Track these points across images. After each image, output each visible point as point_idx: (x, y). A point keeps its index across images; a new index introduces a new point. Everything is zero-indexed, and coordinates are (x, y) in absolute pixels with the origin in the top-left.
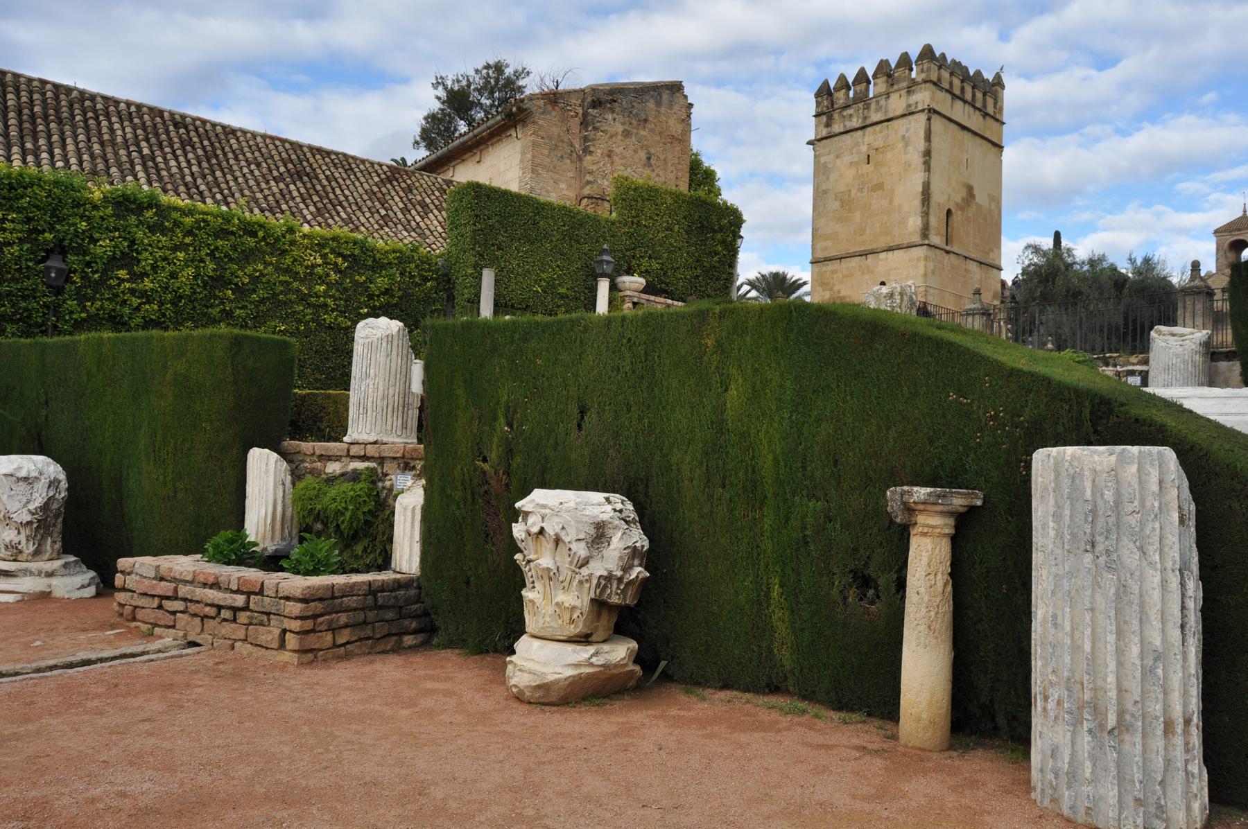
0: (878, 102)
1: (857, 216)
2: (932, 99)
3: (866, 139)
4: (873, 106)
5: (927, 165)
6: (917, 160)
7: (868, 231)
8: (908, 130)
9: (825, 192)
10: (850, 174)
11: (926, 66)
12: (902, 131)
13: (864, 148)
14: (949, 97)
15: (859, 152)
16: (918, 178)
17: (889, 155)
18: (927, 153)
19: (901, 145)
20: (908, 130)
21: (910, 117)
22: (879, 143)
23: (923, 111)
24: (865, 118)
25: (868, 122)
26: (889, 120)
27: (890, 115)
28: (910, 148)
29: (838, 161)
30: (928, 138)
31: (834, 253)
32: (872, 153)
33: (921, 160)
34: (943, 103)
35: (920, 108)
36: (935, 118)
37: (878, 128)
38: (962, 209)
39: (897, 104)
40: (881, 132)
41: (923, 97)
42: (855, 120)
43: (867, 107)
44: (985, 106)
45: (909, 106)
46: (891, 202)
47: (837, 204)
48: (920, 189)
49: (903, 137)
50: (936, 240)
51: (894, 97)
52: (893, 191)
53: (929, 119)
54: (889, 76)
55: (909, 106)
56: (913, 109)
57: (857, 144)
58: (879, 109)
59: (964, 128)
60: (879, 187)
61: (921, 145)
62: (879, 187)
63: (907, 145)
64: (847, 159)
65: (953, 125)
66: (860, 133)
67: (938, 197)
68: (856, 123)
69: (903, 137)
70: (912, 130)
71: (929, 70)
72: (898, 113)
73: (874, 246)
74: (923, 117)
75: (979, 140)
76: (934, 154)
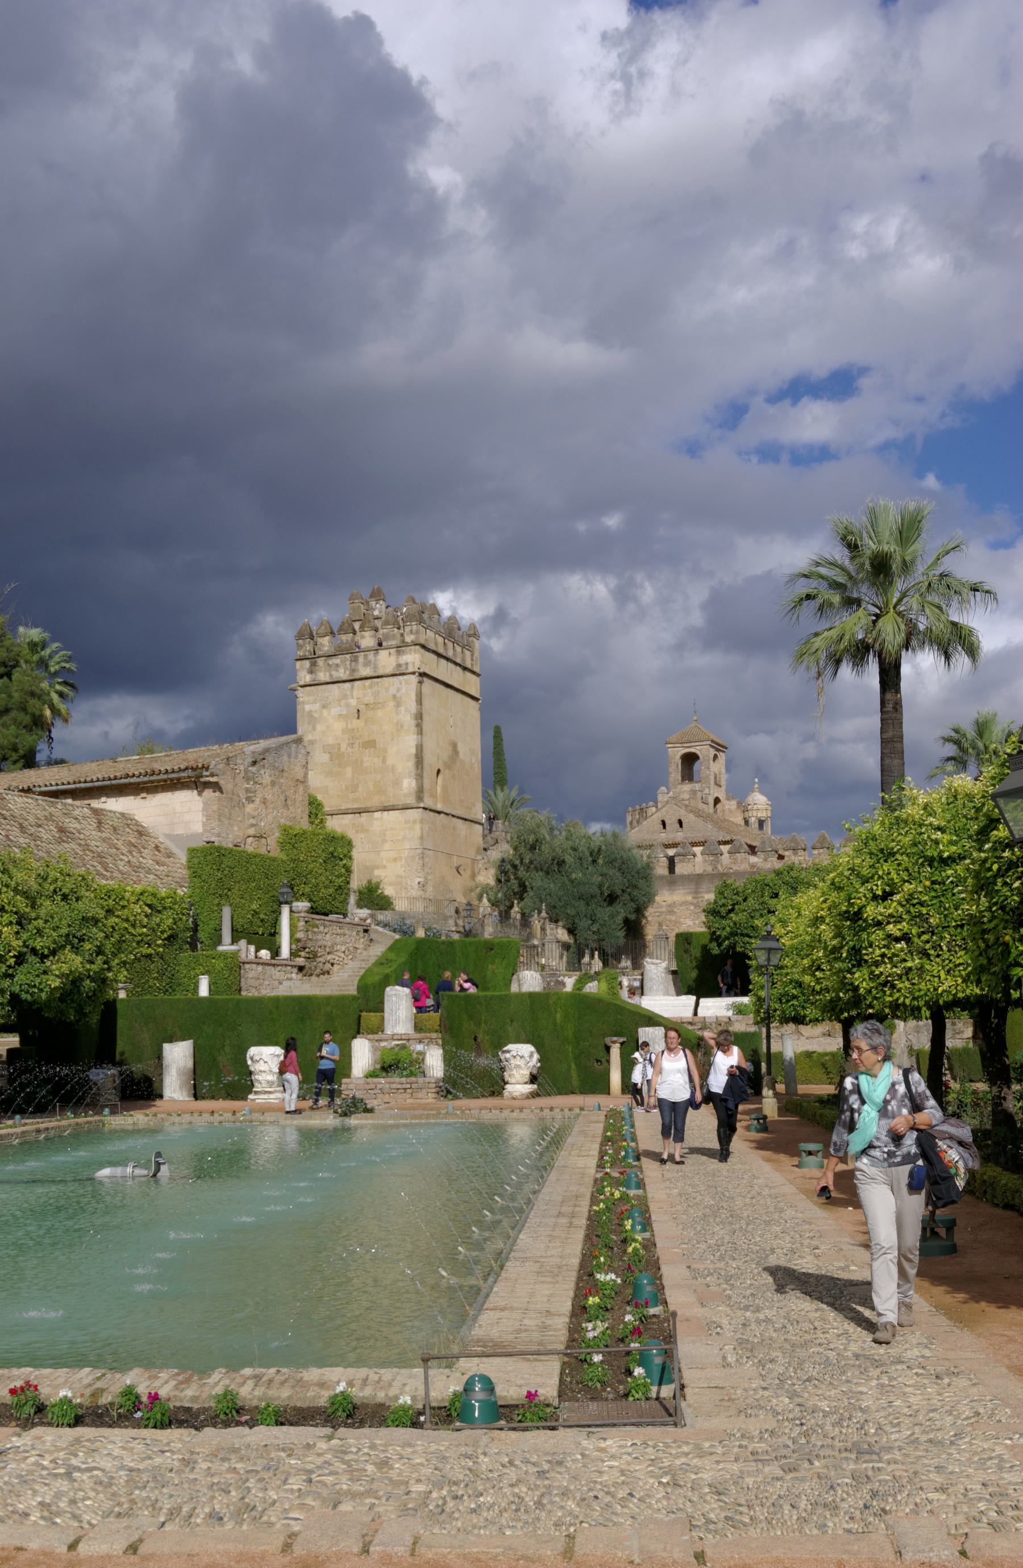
0: (366, 656)
1: (349, 771)
3: (355, 693)
4: (361, 659)
5: (419, 726)
6: (409, 721)
7: (361, 789)
8: (398, 690)
10: (338, 726)
11: (414, 627)
12: (392, 691)
13: (353, 702)
15: (348, 705)
16: (409, 742)
17: (380, 713)
18: (419, 717)
19: (392, 704)
20: (398, 690)
21: (401, 677)
22: (369, 699)
23: (414, 673)
24: (353, 671)
25: (357, 676)
26: (378, 677)
27: (380, 672)
28: (402, 709)
29: (325, 712)
30: (419, 701)
32: (362, 708)
33: (413, 722)
35: (411, 670)
36: (425, 679)
37: (368, 682)
39: (386, 661)
40: (371, 687)
41: (413, 659)
42: (342, 670)
43: (355, 660)
44: (464, 660)
45: (399, 666)
46: (384, 761)
47: (326, 757)
48: (413, 751)
49: (394, 696)
50: (428, 802)
51: (383, 654)
52: (385, 750)
53: (420, 682)
55: (399, 666)
56: (403, 670)
57: (345, 697)
58: (367, 663)
61: (413, 707)
62: (371, 744)
63: (398, 705)
64: (335, 711)
66: (347, 685)
67: (431, 761)
68: (342, 674)
69: (394, 696)
70: (403, 691)
71: (417, 632)
72: (389, 670)
74: (414, 679)
75: (460, 696)
76: (425, 717)
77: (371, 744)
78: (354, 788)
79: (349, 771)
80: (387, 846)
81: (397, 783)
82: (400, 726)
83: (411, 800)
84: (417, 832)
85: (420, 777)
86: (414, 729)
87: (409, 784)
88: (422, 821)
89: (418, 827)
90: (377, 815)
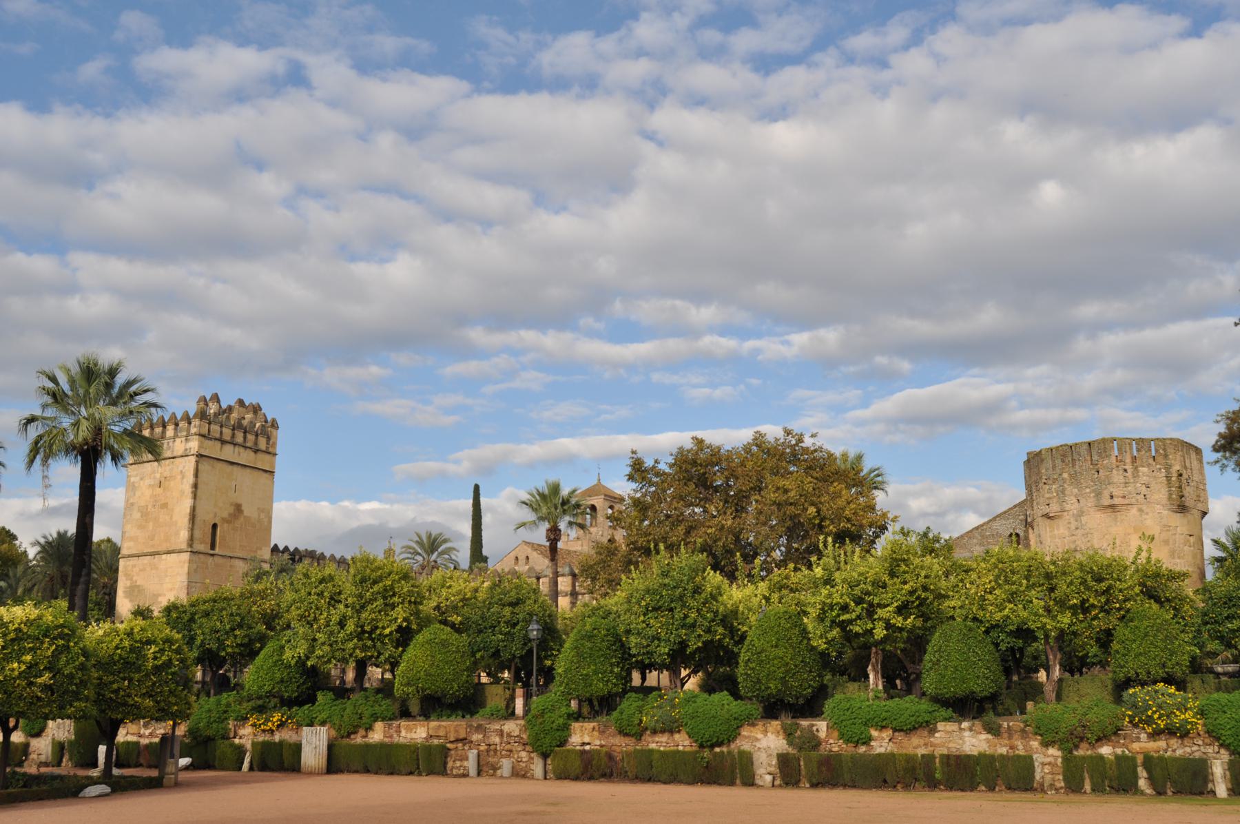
2: (200, 447)
6: (188, 489)
9: (132, 504)
10: (148, 493)
13: (158, 476)
14: (218, 444)
16: (187, 503)
17: (172, 484)
18: (195, 486)
22: (167, 474)
30: (196, 475)
31: (135, 552)
34: (213, 449)
38: (228, 522)
39: (179, 446)
51: (178, 440)
54: (177, 425)
57: (154, 472)
59: (232, 463)
60: (165, 506)
61: (190, 479)
62: (165, 506)
64: (148, 481)
65: (219, 465)
72: (180, 453)
73: (159, 549)
74: (193, 459)
77: (165, 506)
78: (152, 538)
79: (150, 526)
80: (167, 580)
81: (177, 534)
82: (182, 492)
83: (184, 546)
84: (186, 569)
85: (192, 529)
86: (190, 495)
87: (184, 534)
88: (190, 561)
89: (186, 565)
90: (164, 556)
